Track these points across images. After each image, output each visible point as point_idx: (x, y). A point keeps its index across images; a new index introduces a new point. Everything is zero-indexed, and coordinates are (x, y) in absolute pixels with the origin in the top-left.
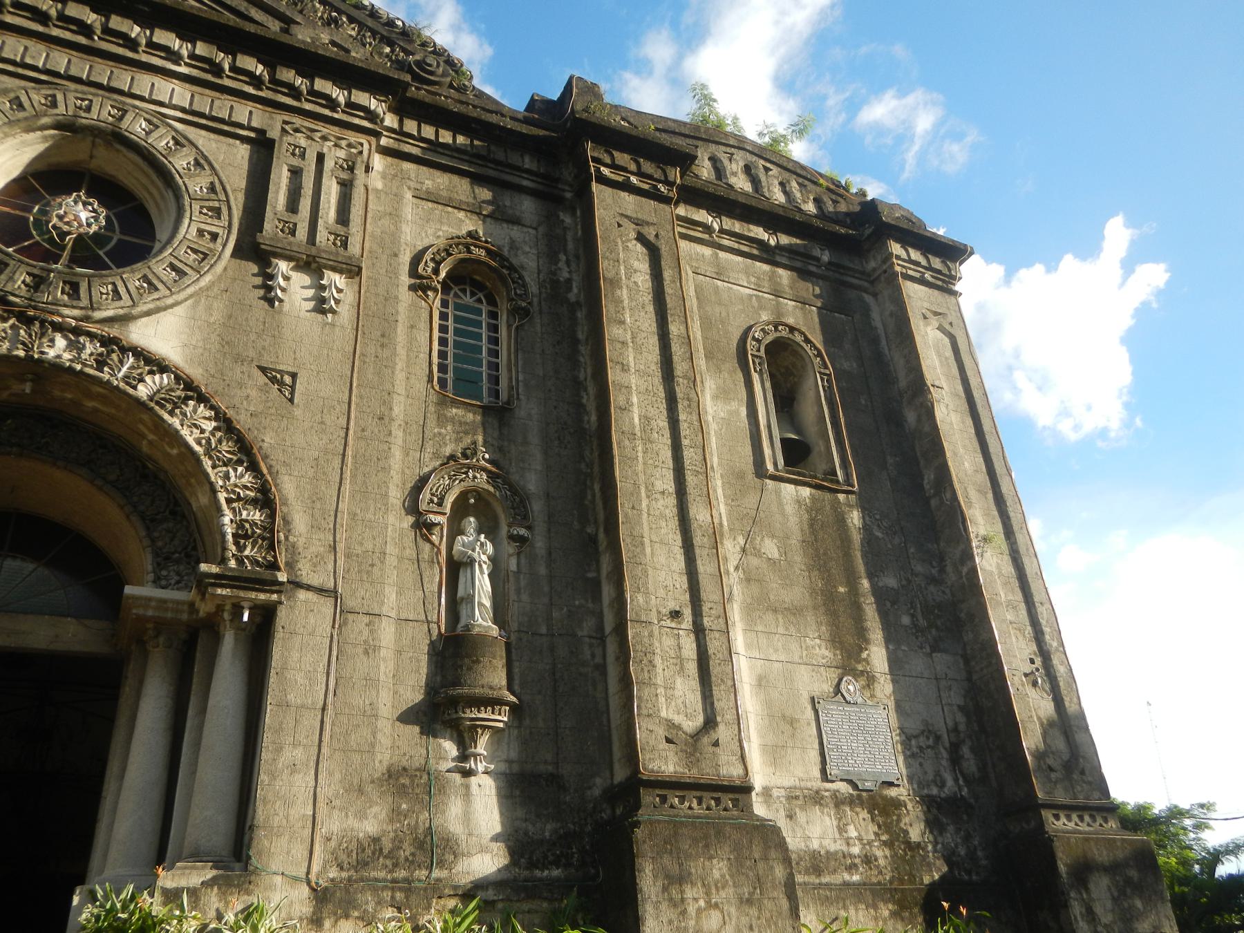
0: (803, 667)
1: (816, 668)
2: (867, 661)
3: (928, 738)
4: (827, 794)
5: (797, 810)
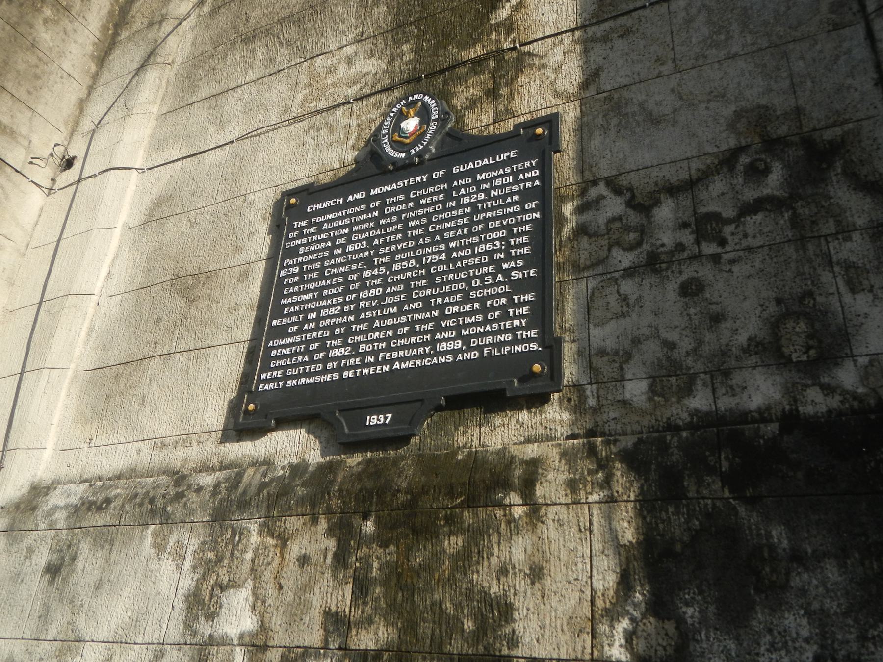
1: (318, 120)
2: (509, 26)
3: (757, 172)
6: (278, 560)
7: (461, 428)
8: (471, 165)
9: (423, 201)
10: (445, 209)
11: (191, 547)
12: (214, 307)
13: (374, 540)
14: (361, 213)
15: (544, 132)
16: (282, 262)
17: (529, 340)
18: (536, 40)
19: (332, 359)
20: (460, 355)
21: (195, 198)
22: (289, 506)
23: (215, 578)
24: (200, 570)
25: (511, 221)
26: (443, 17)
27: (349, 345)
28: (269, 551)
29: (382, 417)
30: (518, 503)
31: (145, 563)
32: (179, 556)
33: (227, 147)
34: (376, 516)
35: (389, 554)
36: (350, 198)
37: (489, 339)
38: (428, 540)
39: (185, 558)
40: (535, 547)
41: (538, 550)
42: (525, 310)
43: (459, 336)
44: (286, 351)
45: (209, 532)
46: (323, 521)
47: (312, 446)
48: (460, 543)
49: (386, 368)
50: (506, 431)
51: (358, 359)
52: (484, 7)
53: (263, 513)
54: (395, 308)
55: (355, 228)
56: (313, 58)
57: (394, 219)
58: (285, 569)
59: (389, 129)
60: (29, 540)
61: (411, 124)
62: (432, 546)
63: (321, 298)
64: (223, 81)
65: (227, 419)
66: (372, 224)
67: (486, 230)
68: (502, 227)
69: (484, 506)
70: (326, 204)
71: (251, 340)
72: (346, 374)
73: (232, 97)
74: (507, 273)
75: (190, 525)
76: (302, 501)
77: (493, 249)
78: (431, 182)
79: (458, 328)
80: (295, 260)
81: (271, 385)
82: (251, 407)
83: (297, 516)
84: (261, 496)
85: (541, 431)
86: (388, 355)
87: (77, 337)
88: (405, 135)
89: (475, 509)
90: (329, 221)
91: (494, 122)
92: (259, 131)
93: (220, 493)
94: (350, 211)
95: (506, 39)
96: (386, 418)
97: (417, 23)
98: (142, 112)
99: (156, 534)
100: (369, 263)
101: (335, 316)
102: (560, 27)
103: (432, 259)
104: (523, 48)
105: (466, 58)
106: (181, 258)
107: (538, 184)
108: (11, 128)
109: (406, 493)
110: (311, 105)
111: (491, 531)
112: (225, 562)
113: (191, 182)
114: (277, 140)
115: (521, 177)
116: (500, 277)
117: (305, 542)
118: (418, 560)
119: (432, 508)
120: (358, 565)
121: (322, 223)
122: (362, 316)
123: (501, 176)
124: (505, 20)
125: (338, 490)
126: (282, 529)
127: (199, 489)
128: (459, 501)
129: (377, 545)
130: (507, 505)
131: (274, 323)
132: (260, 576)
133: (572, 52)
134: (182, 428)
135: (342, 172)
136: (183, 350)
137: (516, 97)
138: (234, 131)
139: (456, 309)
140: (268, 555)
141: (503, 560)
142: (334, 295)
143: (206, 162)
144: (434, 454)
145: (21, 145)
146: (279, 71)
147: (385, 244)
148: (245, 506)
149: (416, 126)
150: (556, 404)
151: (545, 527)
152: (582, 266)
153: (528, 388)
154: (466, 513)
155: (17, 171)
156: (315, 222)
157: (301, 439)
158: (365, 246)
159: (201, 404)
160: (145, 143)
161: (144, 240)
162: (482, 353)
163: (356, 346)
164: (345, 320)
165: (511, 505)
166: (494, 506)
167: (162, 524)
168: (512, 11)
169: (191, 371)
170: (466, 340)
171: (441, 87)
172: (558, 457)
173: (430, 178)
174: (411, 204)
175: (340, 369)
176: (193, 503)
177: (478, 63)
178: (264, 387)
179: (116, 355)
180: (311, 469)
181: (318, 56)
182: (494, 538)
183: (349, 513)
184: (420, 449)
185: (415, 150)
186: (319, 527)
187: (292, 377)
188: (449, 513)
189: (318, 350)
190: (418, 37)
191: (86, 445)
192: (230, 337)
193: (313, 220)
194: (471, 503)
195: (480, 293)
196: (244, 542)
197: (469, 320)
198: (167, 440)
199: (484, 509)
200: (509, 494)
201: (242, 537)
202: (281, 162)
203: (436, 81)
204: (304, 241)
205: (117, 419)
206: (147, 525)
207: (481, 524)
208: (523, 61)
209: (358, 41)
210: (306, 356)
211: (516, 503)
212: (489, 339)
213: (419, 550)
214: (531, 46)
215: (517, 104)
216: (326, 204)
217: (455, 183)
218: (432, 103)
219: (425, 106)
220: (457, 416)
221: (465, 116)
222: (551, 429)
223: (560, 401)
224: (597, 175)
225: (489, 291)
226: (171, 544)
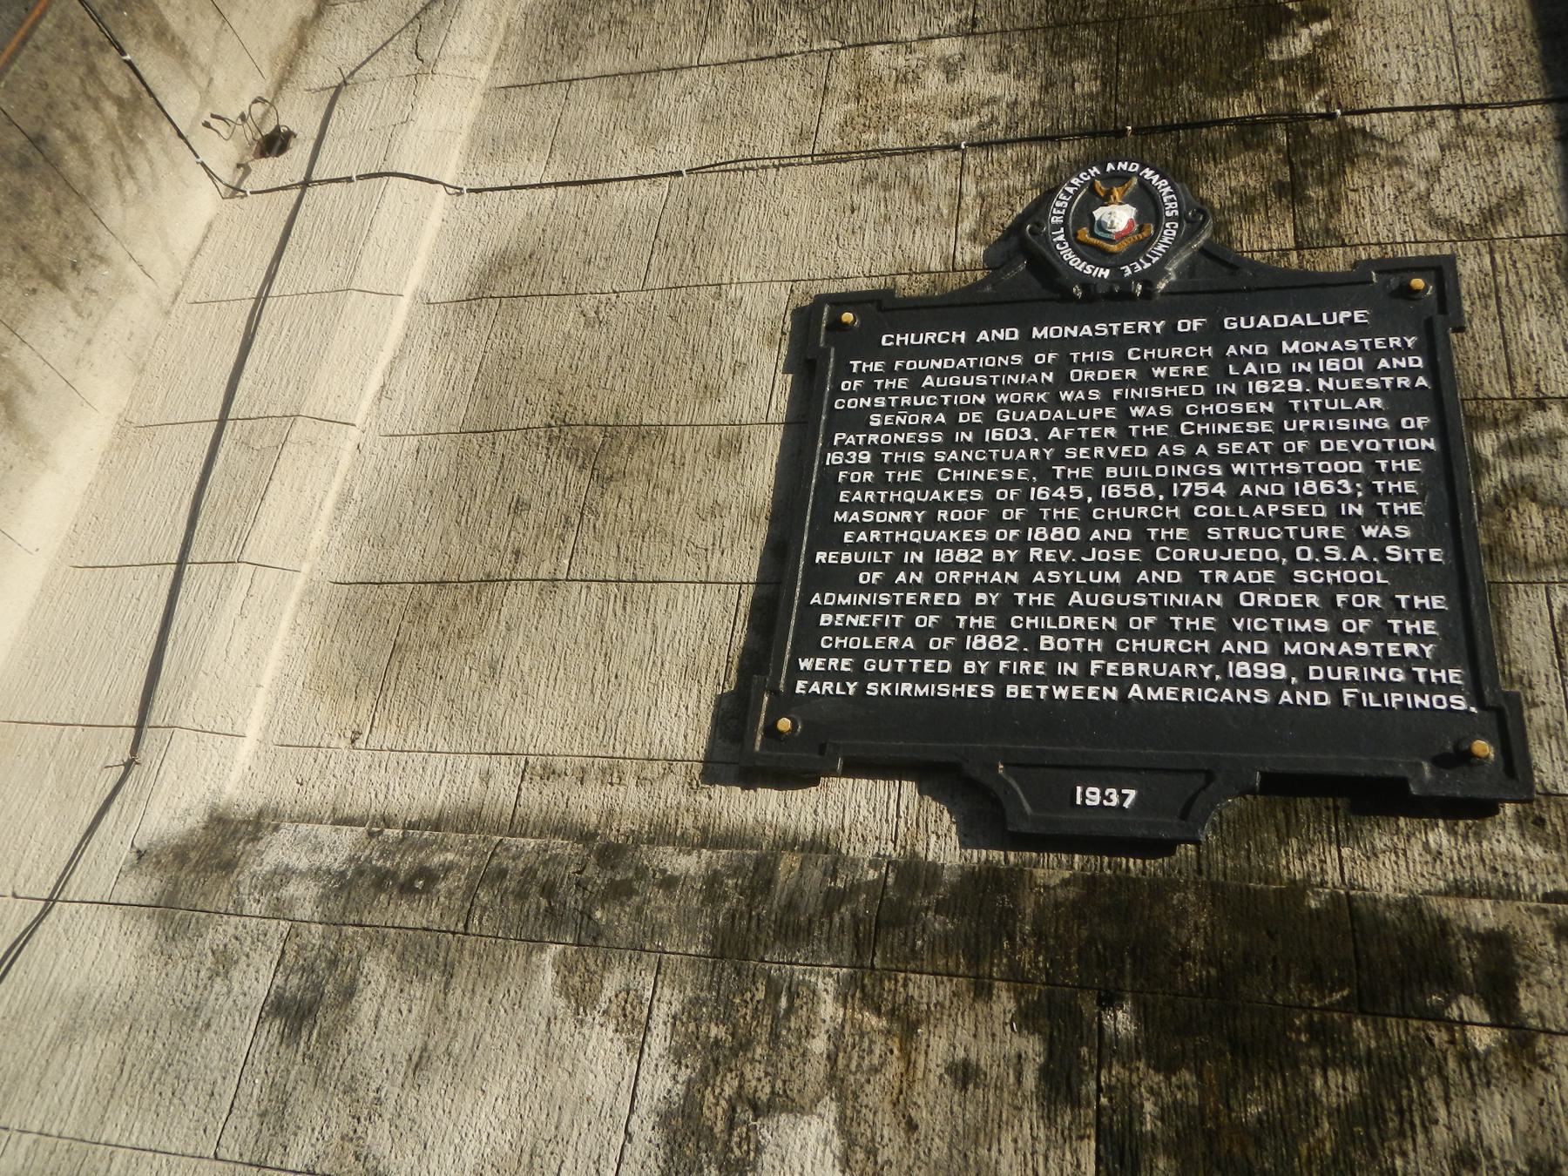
0: (795, 186)
1: (885, 168)
2: (1311, 71)
4: (687, 864)
5: (376, 971)
6: (895, 1066)
7: (1294, 842)
8: (1264, 321)
9: (1159, 372)
10: (1212, 397)
11: (664, 1007)
12: (661, 498)
13: (1138, 1053)
14: (1013, 369)
15: (1426, 289)
16: (829, 439)
17: (1449, 689)
18: (1379, 111)
19: (975, 655)
20: (1286, 693)
21: (593, 270)
22: (913, 950)
23: (736, 1083)
24: (694, 1062)
26: (1160, 27)
28: (872, 1042)
29: (1112, 792)
30: (1480, 1021)
31: (543, 1027)
32: (633, 1024)
33: (665, 181)
34: (1136, 1002)
35: (1179, 1088)
36: (983, 336)
37: (1351, 672)
38: (1272, 1069)
39: (647, 1028)
40: (1535, 1118)
41: (1542, 1124)
42: (1428, 626)
43: (1278, 655)
44: (859, 621)
45: (706, 980)
46: (1004, 995)
47: (932, 827)
48: (1353, 1087)
50: (1402, 862)
51: (1038, 665)
52: (1251, 27)
53: (845, 956)
54: (1117, 575)
55: (1002, 398)
56: (863, 45)
57: (1095, 395)
58: (918, 1087)
59: (1066, 218)
60: (220, 933)
61: (1119, 216)
62: (1285, 1085)
63: (931, 523)
64: (647, 50)
65: (712, 740)
66: (1041, 397)
67: (1315, 452)
68: (1351, 454)
69: (1397, 1016)
70: (930, 337)
71: (757, 584)
72: (1011, 690)
73: (670, 87)
74: (1376, 547)
75: (653, 959)
76: (944, 944)
77: (1336, 493)
78: (1171, 337)
79: (1277, 639)
80: (861, 437)
81: (828, 686)
82: (784, 724)
83: (935, 974)
84: (837, 919)
85: (1482, 873)
86: (1111, 666)
87: (316, 508)
88: (1108, 236)
89: (1379, 1019)
90: (936, 373)
91: (1299, 247)
92: (741, 165)
93: (725, 898)
94: (987, 361)
95: (1308, 97)
96: (1123, 797)
97: (1103, 24)
98: (456, 73)
99: (565, 967)
100: (1042, 472)
101: (969, 566)
102: (1425, 96)
103: (1193, 489)
104: (1348, 119)
105: (1222, 115)
106: (568, 387)
107: (1425, 383)
108: (183, 43)
109: (1207, 962)
110: (865, 137)
111: (1423, 1070)
112: (759, 1051)
113: (581, 236)
114: (789, 189)
115: (1384, 363)
116: (1359, 552)
117: (963, 1035)
118: (1253, 1110)
119: (1275, 1003)
120: (1104, 1100)
121: (923, 374)
122: (1039, 577)
123: (1337, 353)
124: (1302, 59)
125: (1033, 933)
126: (900, 999)
127: (669, 883)
128: (1337, 996)
129: (1148, 1066)
130: (1454, 1021)
131: (821, 556)
132: (854, 1093)
133: (1458, 146)
134: (597, 742)
135: (953, 282)
136: (589, 577)
137: (1344, 208)
138: (680, 154)
139: (1264, 598)
140: (871, 1052)
141: (1462, 1136)
142: (963, 525)
143: (616, 202)
144: (1248, 888)
145: (195, 82)
146: (781, 56)
147: (1077, 441)
148: (796, 936)
149: (1130, 223)
150: (1510, 825)
151: (1552, 1080)
152: (1532, 560)
153: (1455, 785)
154: (1358, 1024)
155: (180, 135)
156: (903, 368)
157: (903, 808)
158: (1029, 437)
159: (642, 700)
160: (462, 139)
161: (471, 334)
163: (1030, 638)
164: (997, 578)
165: (1462, 1023)
166: (1421, 1018)
167: (579, 945)
168: (1314, 47)
169: (611, 624)
170: (1299, 665)
171: (1170, 158)
172: (1549, 936)
173: (1171, 328)
174: (1132, 373)
175: (1000, 681)
176: (660, 909)
177: (1250, 132)
178: (808, 687)
179: (408, 562)
180: (946, 876)
181: (873, 44)
182: (1434, 1088)
183: (1067, 985)
184: (1200, 872)
185: (1132, 268)
186: (997, 1008)
187: (878, 677)
188: (1316, 1018)
189: (940, 630)
190: (1105, 51)
191: (344, 743)
192: (704, 569)
193: (898, 363)
194: (1367, 1004)
195: (1318, 576)
196: (803, 1013)
197: (1297, 625)
198: (559, 764)
199: (1401, 1022)
200: (1456, 998)
201: (797, 1002)
202: (802, 235)
203: (1156, 144)
204: (880, 402)
205: (426, 699)
206: (540, 944)
207: (1397, 1052)
208: (1351, 143)
209: (967, 35)
210: (909, 639)
211: (1474, 1020)
212: (1351, 672)
213: (1252, 1088)
214: (1367, 118)
215: (1346, 220)
216: (930, 337)
217: (1232, 350)
218: (1163, 187)
219: (1145, 185)
220: (1280, 815)
221: (1231, 223)
222: (1505, 874)
223: (1520, 821)
224: (1544, 390)
225: (1338, 575)
226: (609, 991)
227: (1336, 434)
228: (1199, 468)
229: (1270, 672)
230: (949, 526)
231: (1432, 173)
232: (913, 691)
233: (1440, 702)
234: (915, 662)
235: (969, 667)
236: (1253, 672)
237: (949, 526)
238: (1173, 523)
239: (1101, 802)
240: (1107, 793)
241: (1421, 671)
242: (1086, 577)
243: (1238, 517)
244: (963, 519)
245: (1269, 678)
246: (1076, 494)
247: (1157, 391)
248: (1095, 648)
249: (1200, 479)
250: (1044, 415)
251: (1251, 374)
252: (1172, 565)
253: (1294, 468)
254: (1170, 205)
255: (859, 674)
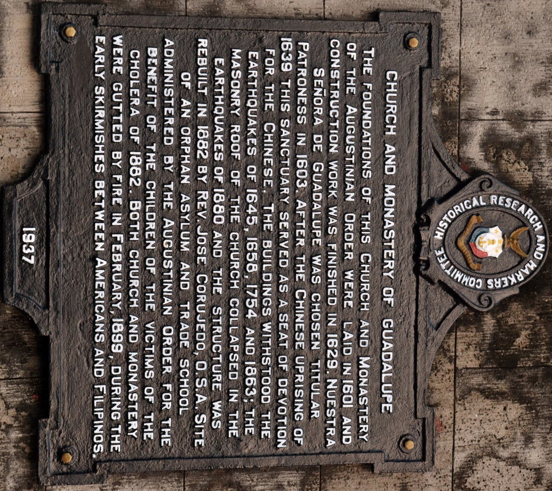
9: (350, 275)
25: (281, 411)
27: (144, 183)
36: (390, 148)
37: (118, 390)
43: (128, 347)
44: (152, 74)
49: (100, 247)
55: (334, 165)
67: (279, 373)
68: (276, 397)
70: (393, 108)
81: (101, 59)
116: (201, 399)
137: (488, 402)
139: (169, 341)
147: (295, 219)
162: (100, 381)
164: (185, 169)
178: (101, 44)
189: (146, 132)
197: (150, 360)
210: (138, 112)
212: (118, 390)
216: (393, 108)
227: (293, 388)
228: (268, 302)
229: (116, 343)
230: (228, 134)
231: (514, 461)
232: (100, 118)
233: (99, 438)
234: (121, 118)
235: (118, 155)
236: (116, 334)
237: (228, 134)
238: (228, 285)
239: (25, 243)
240: (31, 246)
241: (119, 429)
242: (186, 229)
243: (229, 326)
244: (232, 143)
245: (112, 343)
246: (251, 221)
247: (333, 274)
248: (133, 236)
249: (261, 302)
250: (318, 196)
251: (343, 336)
252: (195, 284)
253: (267, 361)
254: (499, 282)
255: (113, 78)
